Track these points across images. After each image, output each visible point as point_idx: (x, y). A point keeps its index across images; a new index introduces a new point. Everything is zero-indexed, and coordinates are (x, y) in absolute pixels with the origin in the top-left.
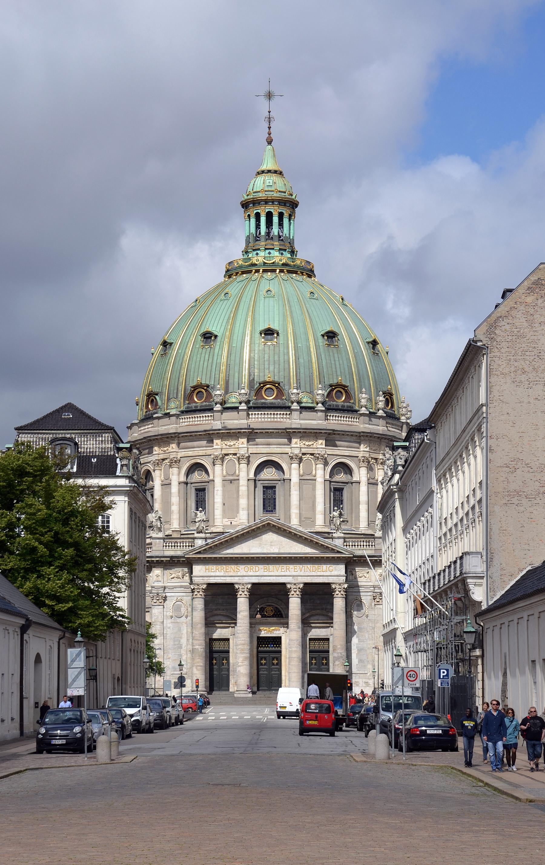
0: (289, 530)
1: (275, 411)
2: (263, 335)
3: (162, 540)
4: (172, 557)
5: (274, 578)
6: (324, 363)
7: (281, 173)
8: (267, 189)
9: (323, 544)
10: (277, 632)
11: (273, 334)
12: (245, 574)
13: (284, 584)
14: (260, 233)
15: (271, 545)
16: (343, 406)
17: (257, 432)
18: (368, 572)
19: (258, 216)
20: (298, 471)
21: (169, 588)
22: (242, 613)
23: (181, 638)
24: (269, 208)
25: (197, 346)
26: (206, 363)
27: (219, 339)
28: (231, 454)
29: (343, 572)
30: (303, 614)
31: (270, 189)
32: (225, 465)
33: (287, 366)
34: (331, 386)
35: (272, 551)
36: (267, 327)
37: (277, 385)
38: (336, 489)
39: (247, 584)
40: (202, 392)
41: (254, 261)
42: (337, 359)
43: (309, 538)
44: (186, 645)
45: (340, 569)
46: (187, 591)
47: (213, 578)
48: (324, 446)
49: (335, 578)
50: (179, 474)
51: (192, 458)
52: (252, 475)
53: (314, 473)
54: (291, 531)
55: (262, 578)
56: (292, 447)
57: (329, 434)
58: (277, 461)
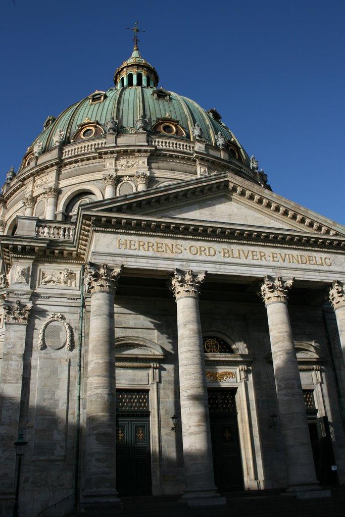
1: (178, 141)
2: (155, 95)
4: (51, 241)
5: (243, 268)
11: (166, 96)
12: (191, 257)
23: (57, 386)
27: (108, 99)
28: (126, 176)
40: (90, 130)
44: (66, 401)
46: (73, 305)
47: (133, 260)
50: (56, 205)
51: (76, 185)
54: (264, 196)
55: (223, 267)
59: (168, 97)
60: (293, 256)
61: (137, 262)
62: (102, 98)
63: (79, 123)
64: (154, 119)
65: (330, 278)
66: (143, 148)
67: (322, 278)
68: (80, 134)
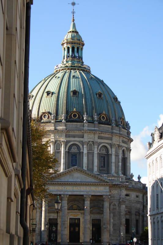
5: (79, 193)
6: (97, 105)
7: (78, 33)
8: (72, 38)
10: (78, 216)
13: (82, 195)
14: (69, 55)
15: (77, 179)
16: (105, 123)
17: (70, 132)
20: (86, 149)
22: (64, 208)
25: (45, 96)
26: (48, 104)
30: (90, 208)
31: (73, 38)
32: (55, 146)
33: (82, 105)
34: (100, 114)
35: (77, 181)
36: (74, 89)
38: (102, 157)
39: (67, 195)
41: (67, 65)
42: (102, 103)
45: (107, 188)
48: (97, 138)
52: (67, 149)
53: (93, 149)
55: (74, 192)
57: (100, 133)
58: (77, 144)
59: (77, 93)
60: (93, 188)
62: (51, 94)
63: (42, 112)
64: (69, 111)
66: (64, 131)
68: (42, 117)
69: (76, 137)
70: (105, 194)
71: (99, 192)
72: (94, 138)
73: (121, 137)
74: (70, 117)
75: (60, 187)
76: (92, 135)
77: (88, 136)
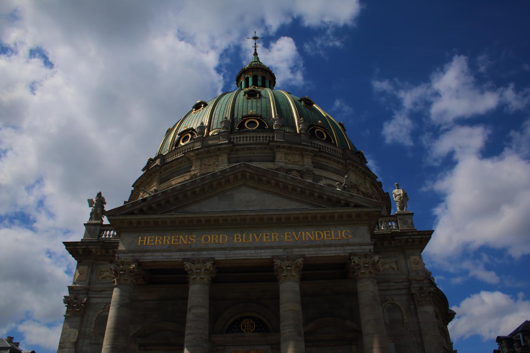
0: (275, 178)
2: (247, 95)
3: (98, 228)
5: (253, 251)
9: (331, 194)
18: (396, 261)
19: (247, 80)
21: (95, 291)
22: (194, 311)
24: (255, 73)
29: (367, 238)
34: (313, 125)
37: (259, 118)
39: (204, 261)
43: (308, 188)
47: (150, 254)
48: (311, 164)
49: (355, 248)
55: (232, 252)
56: (277, 162)
59: (258, 95)
61: (152, 256)
62: (203, 105)
65: (348, 251)
66: (222, 146)
67: (338, 252)
69: (257, 161)
70: (356, 249)
71: (335, 245)
72: (301, 162)
73: (367, 177)
74: (241, 126)
75: (181, 237)
76: (297, 158)
77: (285, 157)
